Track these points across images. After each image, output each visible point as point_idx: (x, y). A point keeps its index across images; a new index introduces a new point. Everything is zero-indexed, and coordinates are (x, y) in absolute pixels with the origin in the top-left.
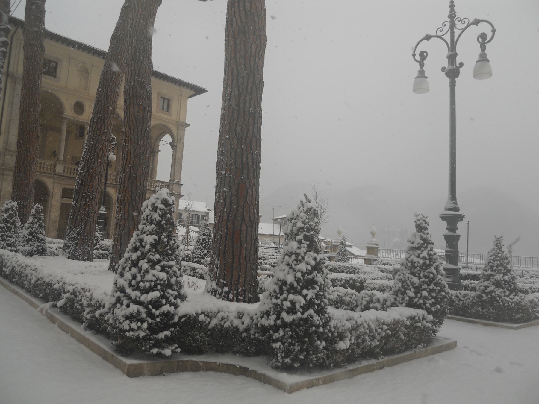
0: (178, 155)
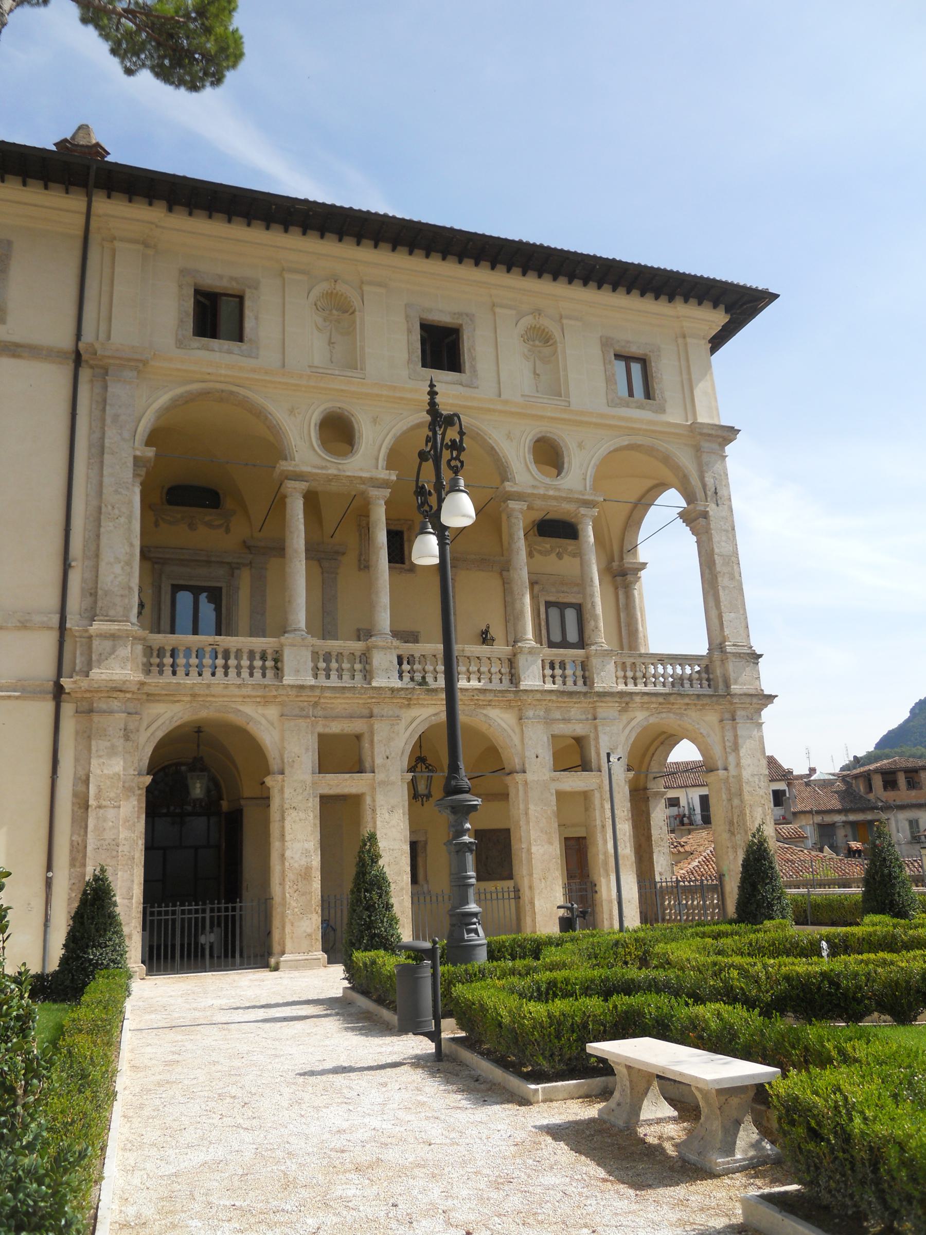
0: (720, 546)
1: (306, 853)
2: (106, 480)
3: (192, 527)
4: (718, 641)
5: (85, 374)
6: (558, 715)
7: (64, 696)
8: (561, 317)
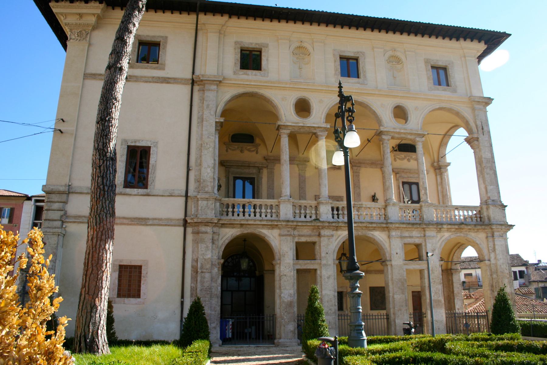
1: (290, 295)
2: (204, 133)
3: (242, 151)
4: (485, 200)
5: (196, 88)
6: (407, 234)
7: (187, 225)
8: (405, 52)
